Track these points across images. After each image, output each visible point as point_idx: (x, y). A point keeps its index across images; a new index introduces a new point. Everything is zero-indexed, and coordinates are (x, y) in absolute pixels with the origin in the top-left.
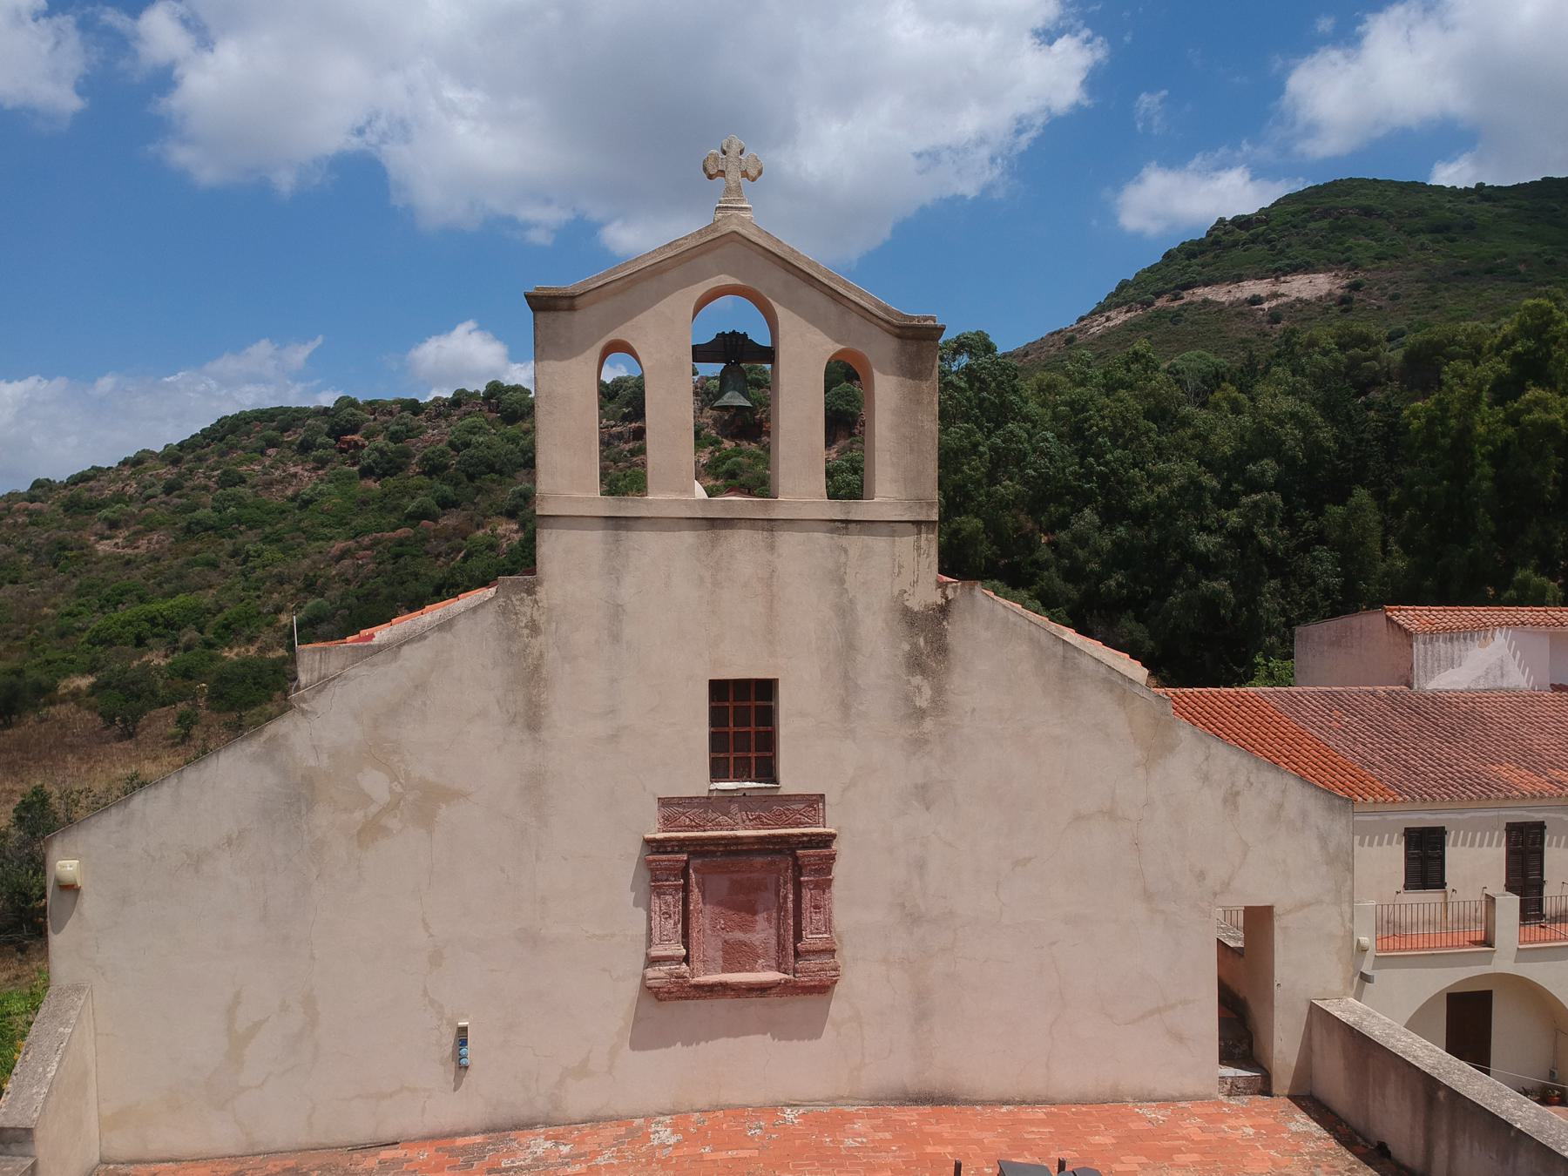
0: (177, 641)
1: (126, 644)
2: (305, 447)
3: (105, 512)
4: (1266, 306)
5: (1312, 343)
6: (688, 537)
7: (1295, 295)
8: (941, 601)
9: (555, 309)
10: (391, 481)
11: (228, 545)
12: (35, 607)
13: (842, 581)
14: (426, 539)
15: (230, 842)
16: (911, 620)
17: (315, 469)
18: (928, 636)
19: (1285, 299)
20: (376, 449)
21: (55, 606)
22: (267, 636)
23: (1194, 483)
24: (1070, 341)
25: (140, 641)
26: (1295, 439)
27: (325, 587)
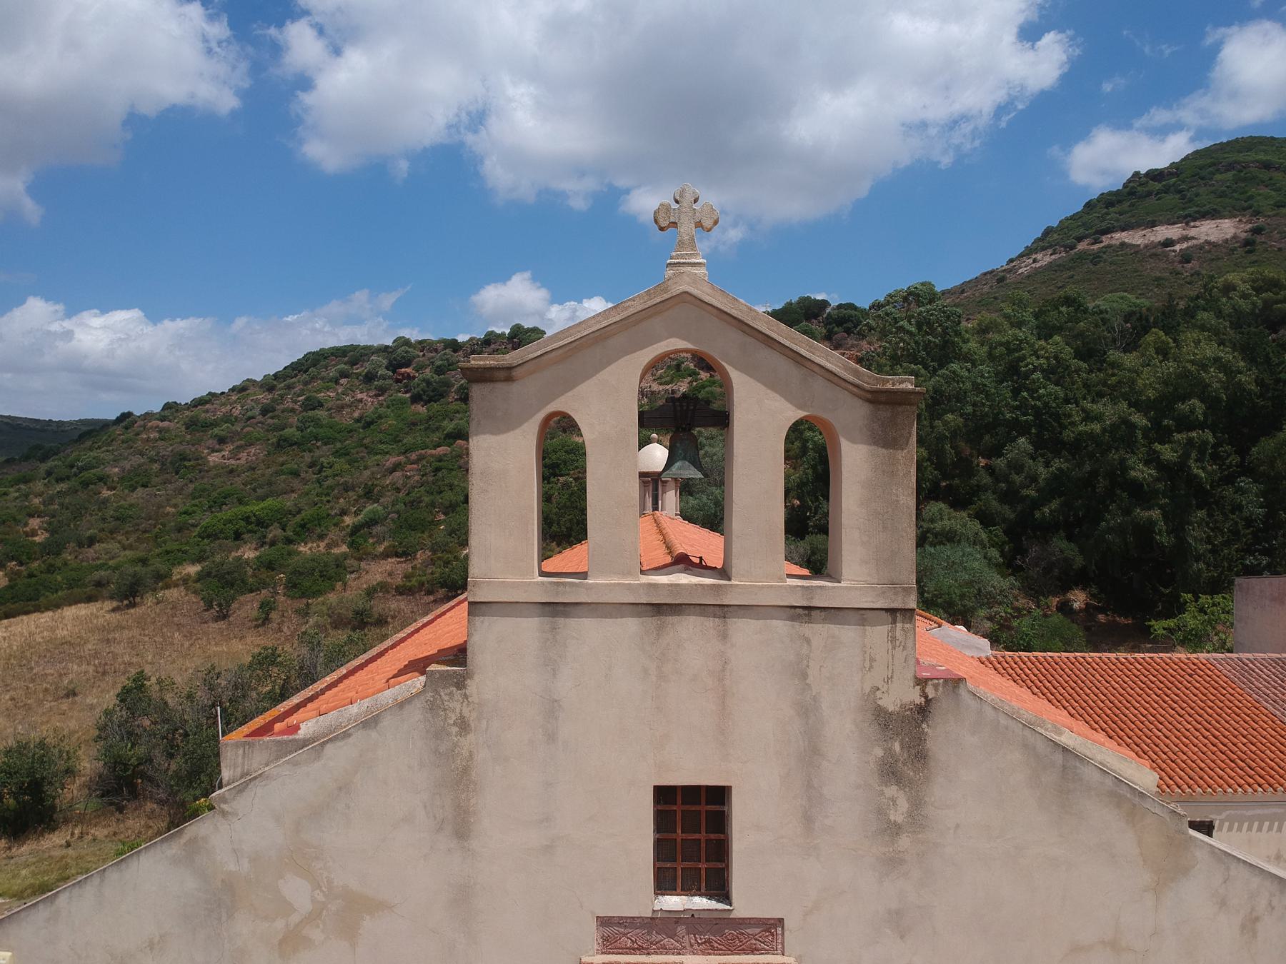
0: (264, 537)
1: (226, 538)
2: (369, 378)
3: (216, 431)
4: (1177, 248)
6: (631, 625)
7: (1203, 238)
8: (920, 700)
9: (492, 380)
11: (308, 457)
12: (160, 506)
13: (804, 676)
15: (151, 946)
16: (884, 721)
17: (377, 396)
18: (907, 734)
19: (1194, 242)
20: (424, 380)
21: (175, 506)
22: (334, 534)
23: (1125, 421)
24: (1001, 280)
25: (238, 536)
26: (1220, 381)
27: (381, 495)
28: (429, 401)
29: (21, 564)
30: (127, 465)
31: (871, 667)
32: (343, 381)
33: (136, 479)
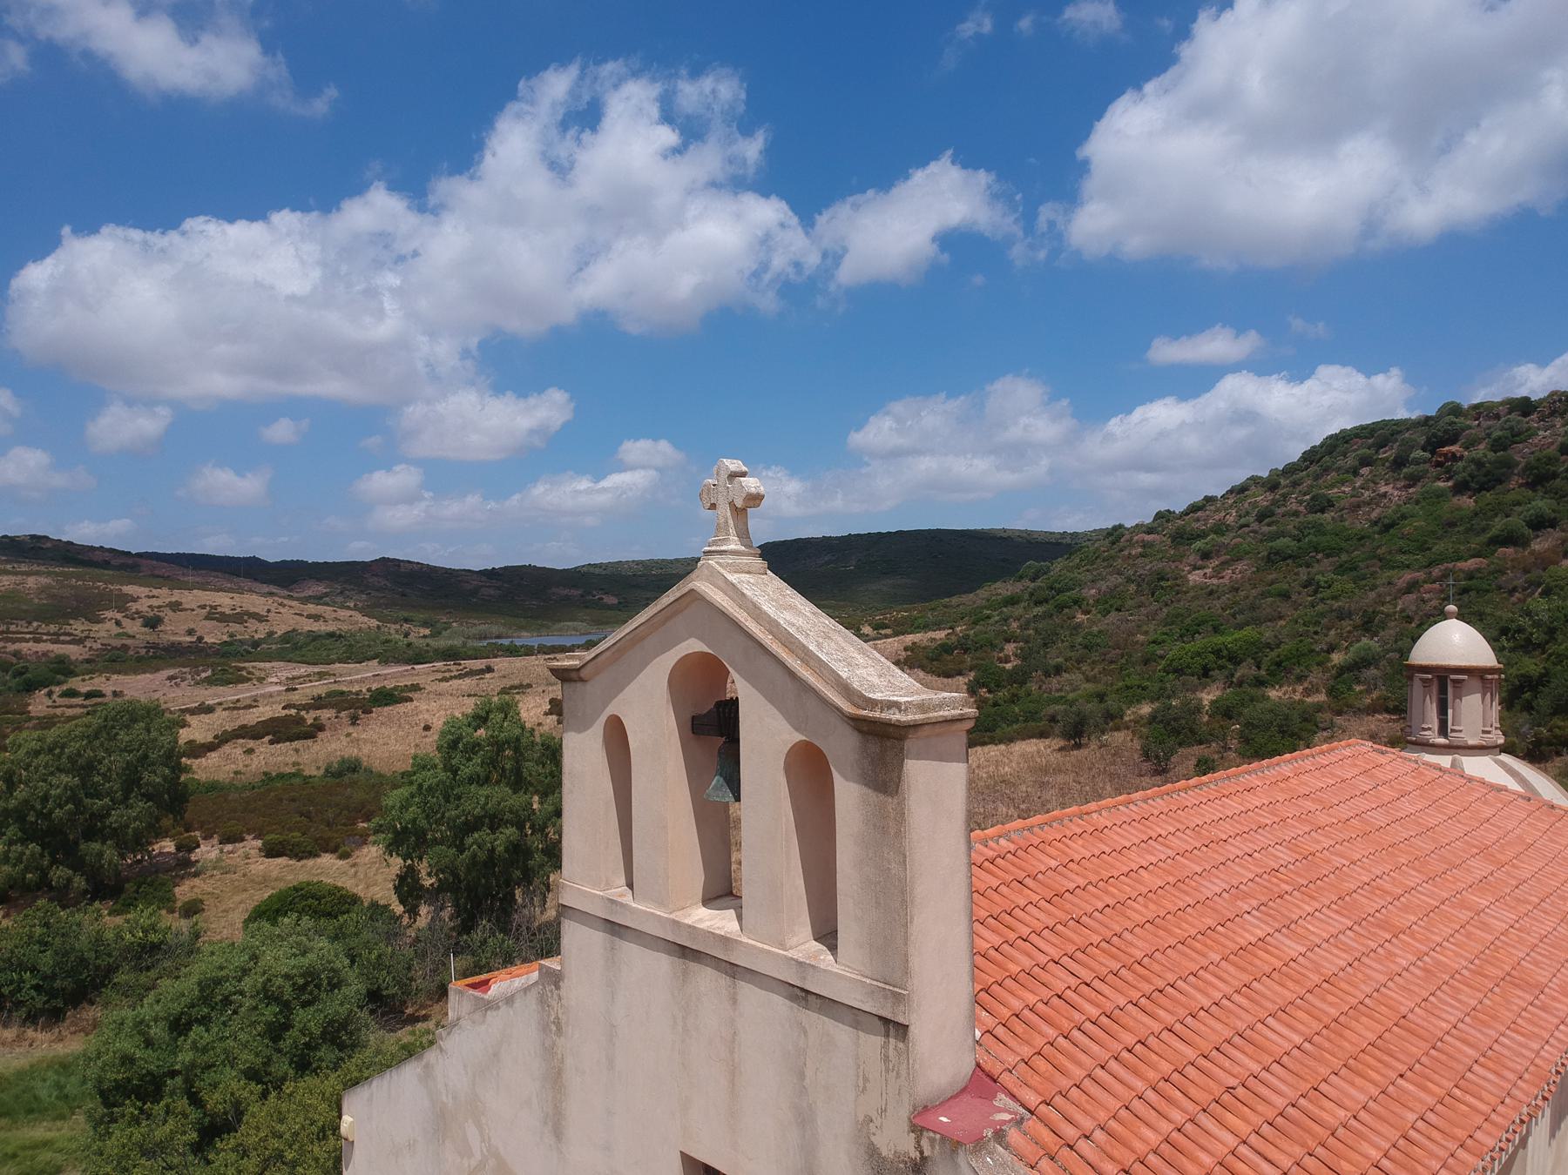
2: (1399, 463)
3: (1199, 544)
8: (915, 1154)
10: (1488, 496)
11: (1303, 574)
14: (1502, 572)
20: (1473, 461)
21: (1146, 633)
22: (1316, 676)
25: (1206, 672)
28: (1479, 491)
29: (990, 692)
30: (1103, 586)
31: (865, 1088)
32: (1365, 471)
33: (1111, 602)
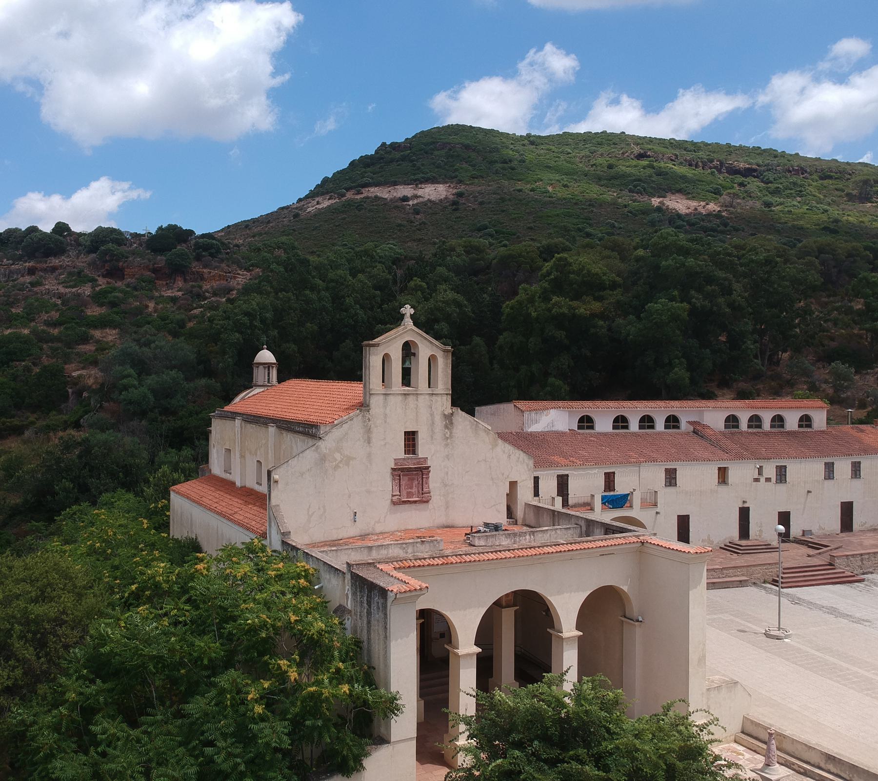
4: (411, 203)
5: (453, 249)
7: (427, 197)
